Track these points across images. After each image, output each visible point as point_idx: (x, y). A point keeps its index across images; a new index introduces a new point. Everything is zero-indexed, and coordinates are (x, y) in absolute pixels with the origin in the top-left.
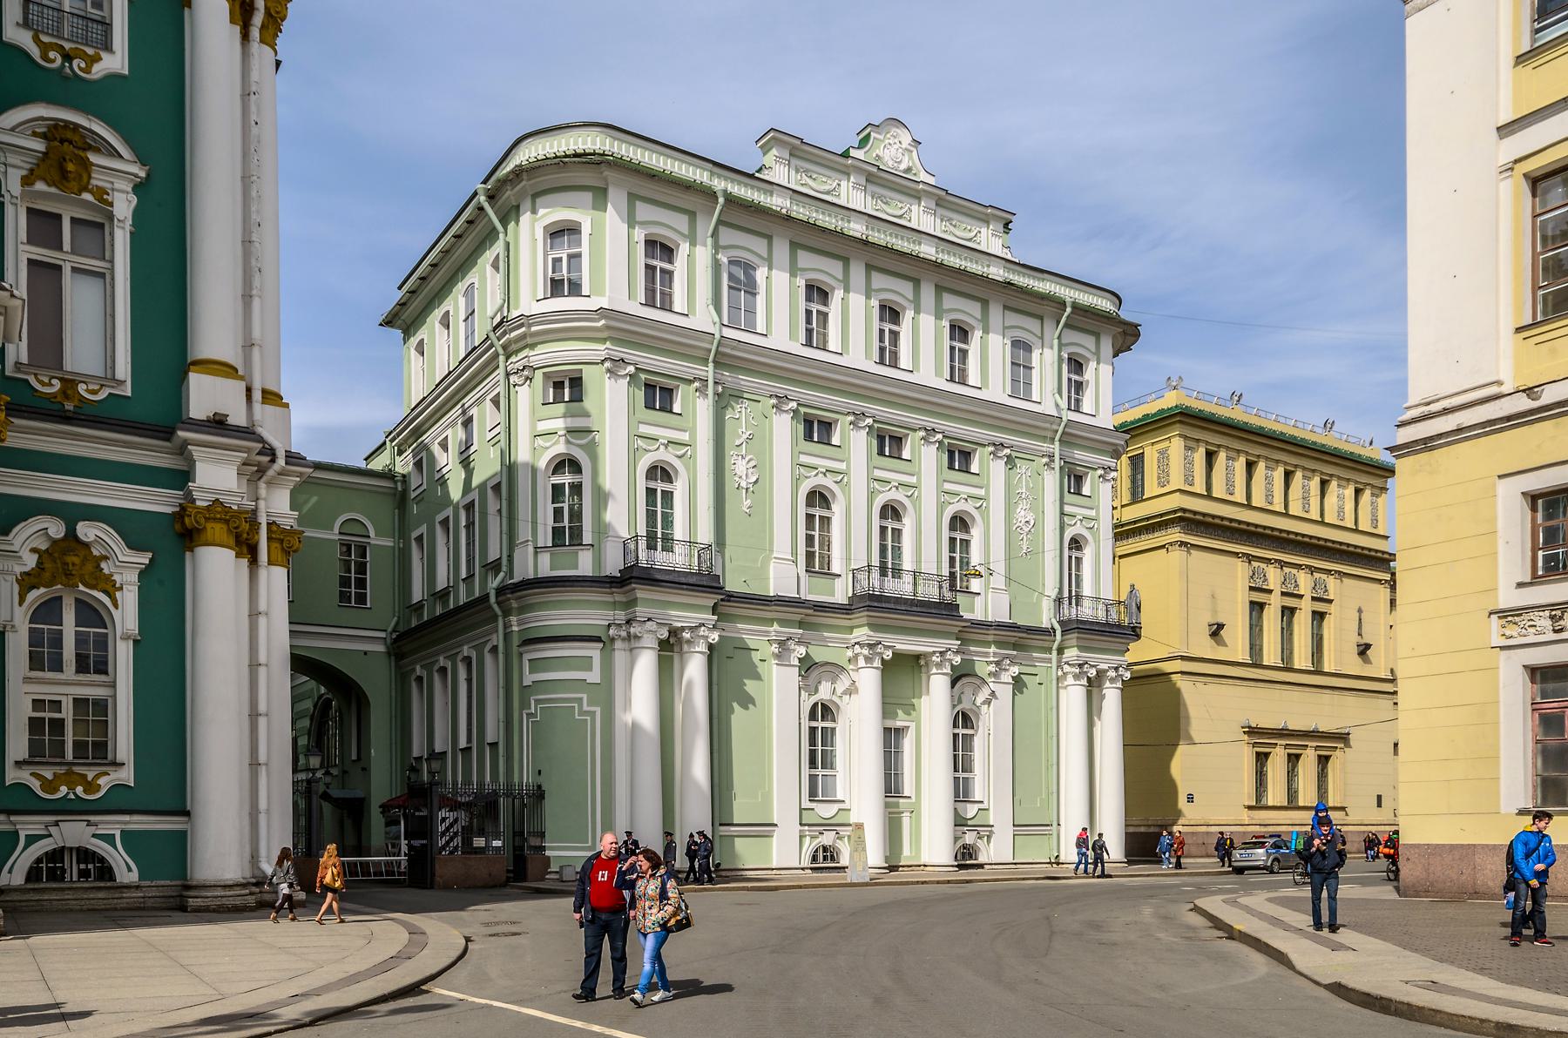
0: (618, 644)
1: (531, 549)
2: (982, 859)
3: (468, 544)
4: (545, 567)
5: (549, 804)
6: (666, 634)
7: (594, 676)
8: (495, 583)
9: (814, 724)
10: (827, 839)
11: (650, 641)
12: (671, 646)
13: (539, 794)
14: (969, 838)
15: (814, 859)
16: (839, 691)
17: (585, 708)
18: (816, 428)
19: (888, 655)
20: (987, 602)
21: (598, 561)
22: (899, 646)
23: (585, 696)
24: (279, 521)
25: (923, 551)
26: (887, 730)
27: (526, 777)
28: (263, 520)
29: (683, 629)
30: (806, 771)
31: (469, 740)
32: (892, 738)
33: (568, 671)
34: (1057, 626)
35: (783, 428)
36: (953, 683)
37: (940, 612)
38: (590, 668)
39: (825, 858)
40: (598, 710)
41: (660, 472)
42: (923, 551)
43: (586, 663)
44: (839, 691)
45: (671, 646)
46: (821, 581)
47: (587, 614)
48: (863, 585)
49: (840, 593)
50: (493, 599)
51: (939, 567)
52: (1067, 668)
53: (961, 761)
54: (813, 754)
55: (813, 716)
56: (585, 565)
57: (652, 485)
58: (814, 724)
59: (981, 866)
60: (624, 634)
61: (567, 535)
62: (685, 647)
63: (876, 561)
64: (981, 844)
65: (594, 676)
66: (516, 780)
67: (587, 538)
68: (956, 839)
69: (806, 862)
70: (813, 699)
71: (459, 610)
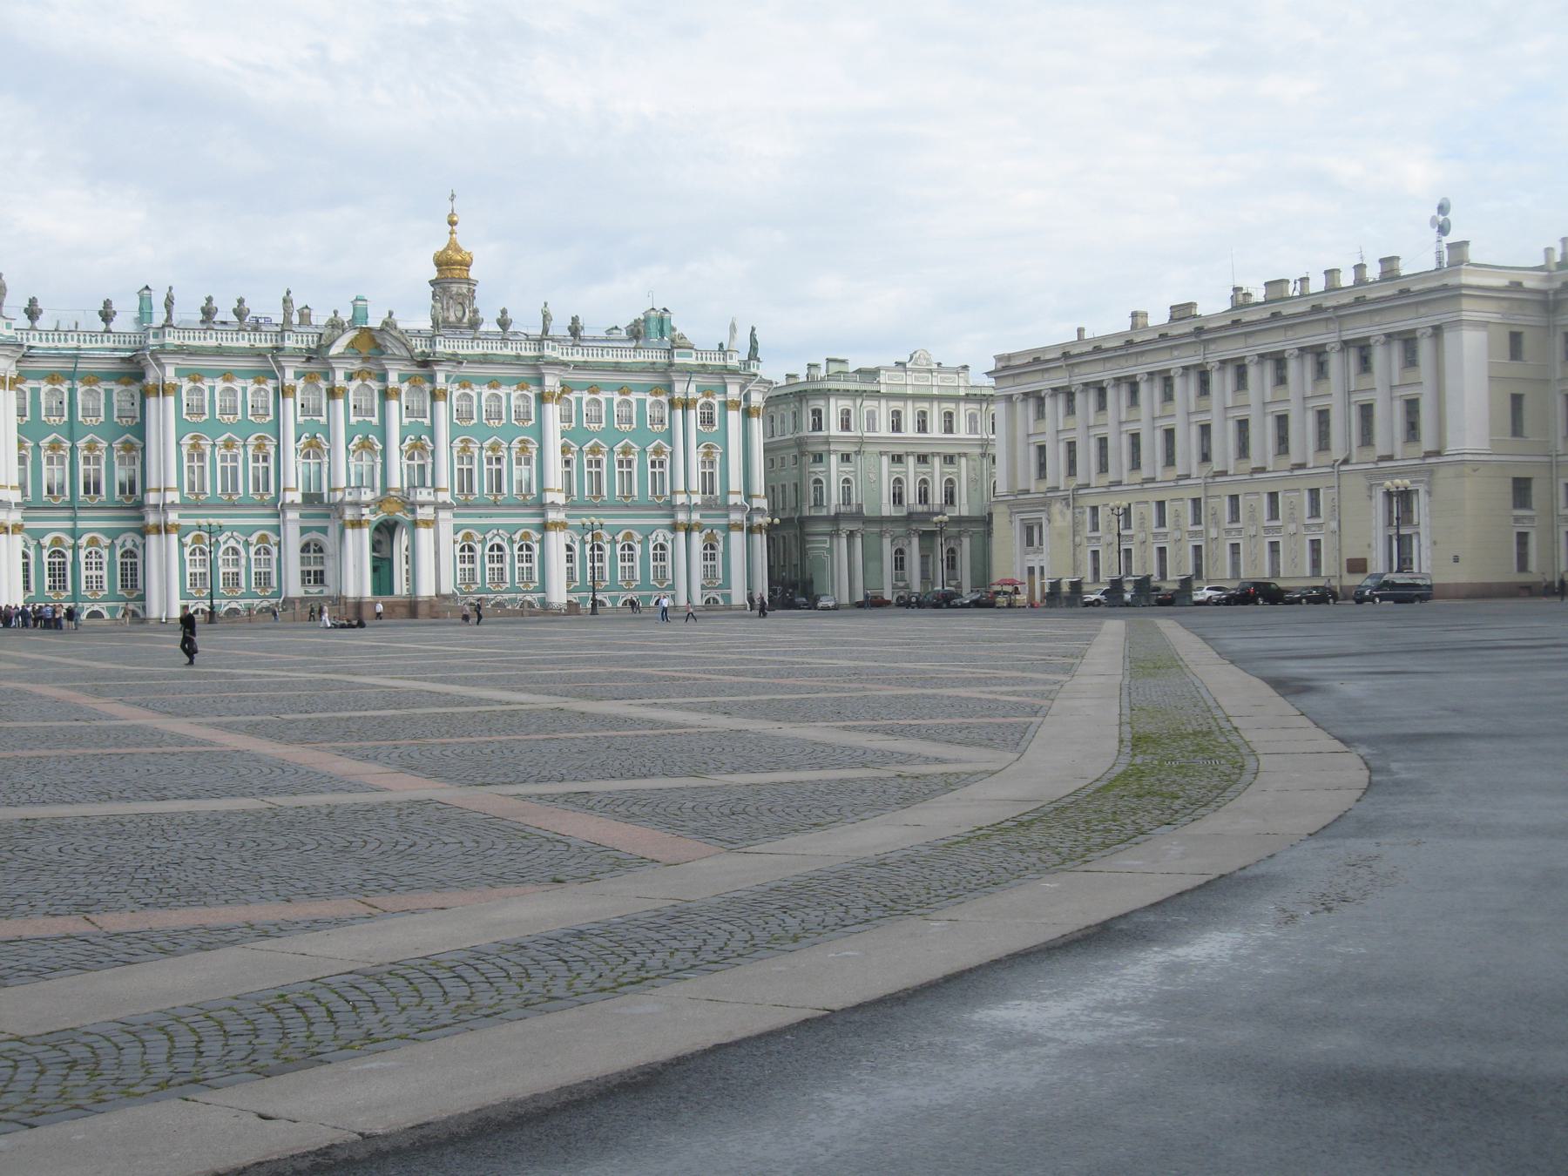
12: (851, 535)
13: (811, 582)
18: (897, 459)
25: (937, 496)
32: (924, 559)
33: (819, 545)
35: (885, 460)
41: (847, 481)
42: (937, 496)
45: (851, 535)
49: (905, 513)
56: (824, 513)
61: (818, 503)
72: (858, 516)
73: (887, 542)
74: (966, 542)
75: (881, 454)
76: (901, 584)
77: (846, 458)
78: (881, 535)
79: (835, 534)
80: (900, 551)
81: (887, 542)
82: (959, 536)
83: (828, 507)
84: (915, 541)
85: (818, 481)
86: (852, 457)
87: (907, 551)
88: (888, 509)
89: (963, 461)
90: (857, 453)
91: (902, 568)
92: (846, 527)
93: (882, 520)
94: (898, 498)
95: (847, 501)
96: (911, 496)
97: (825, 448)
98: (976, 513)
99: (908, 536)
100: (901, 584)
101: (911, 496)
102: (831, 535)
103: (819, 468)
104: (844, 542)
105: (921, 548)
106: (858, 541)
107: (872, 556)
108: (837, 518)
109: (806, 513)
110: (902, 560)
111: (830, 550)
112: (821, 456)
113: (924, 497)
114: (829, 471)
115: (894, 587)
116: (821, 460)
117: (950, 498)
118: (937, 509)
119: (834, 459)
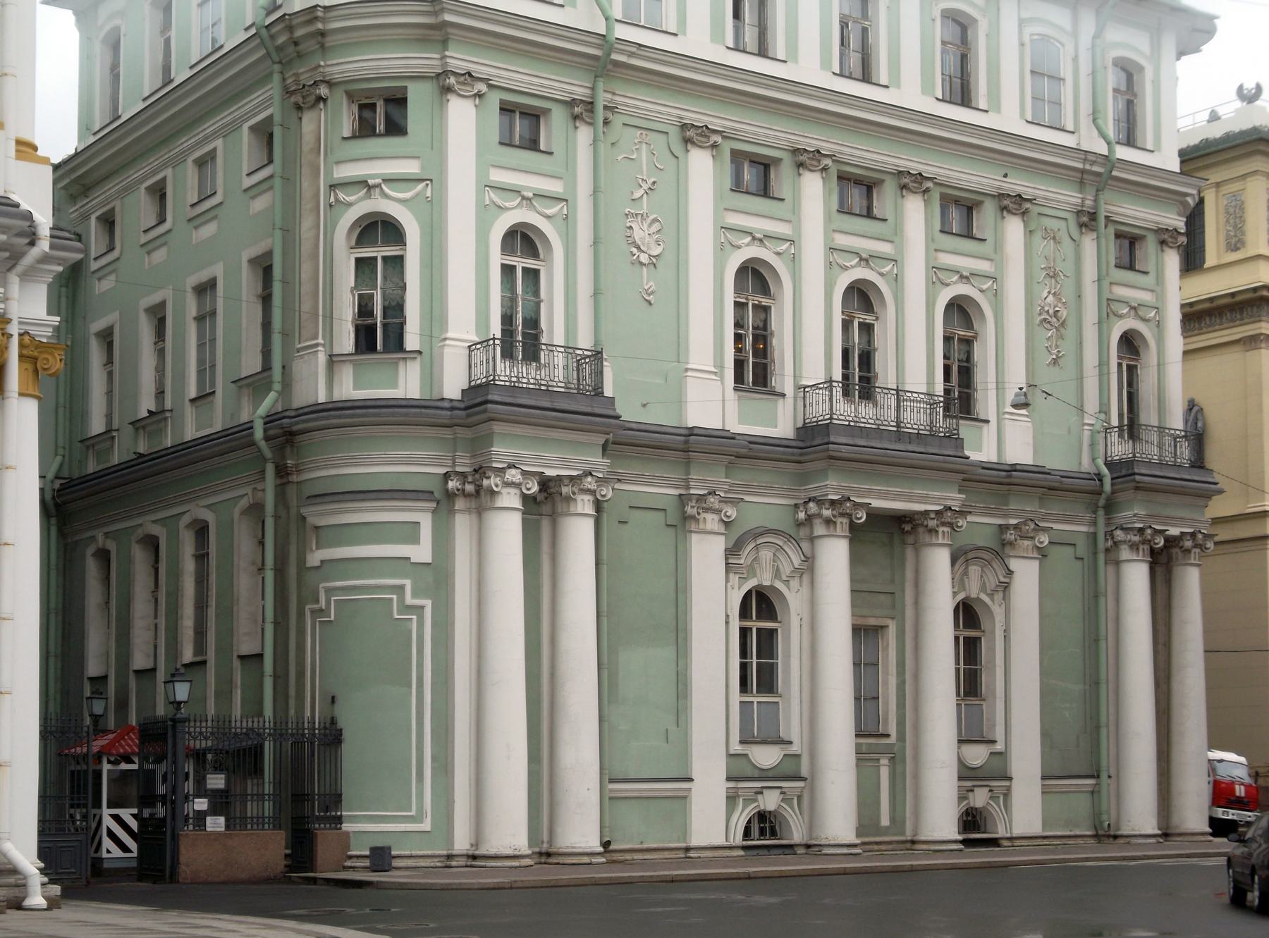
0: (460, 504)
1: (322, 358)
2: (1001, 832)
3: (201, 346)
4: (348, 388)
5: (350, 750)
6: (535, 488)
7: (422, 552)
8: (263, 410)
9: (747, 624)
10: (770, 801)
11: (510, 499)
12: (545, 502)
13: (333, 737)
14: (980, 798)
15: (747, 833)
16: (786, 569)
17: (409, 600)
19: (862, 516)
20: (1001, 439)
21: (432, 375)
22: (876, 503)
23: (408, 583)
24: (34, 331)
25: (912, 362)
26: (857, 630)
27: (313, 712)
28: (14, 329)
29: (559, 478)
30: (736, 696)
31: (200, 647)
33: (380, 547)
34: (1105, 471)
36: (954, 561)
37: (933, 454)
38: (414, 539)
39: (762, 832)
40: (428, 604)
42: (912, 360)
43: (410, 533)
44: (786, 569)
45: (545, 502)
46: (758, 402)
47: (417, 461)
48: (818, 410)
49: (780, 422)
50: (259, 433)
51: (930, 382)
52: (1119, 535)
53: (970, 684)
54: (744, 668)
55: (744, 612)
56: (408, 383)
57: (510, 261)
58: (747, 624)
59: (994, 842)
60: (470, 488)
61: (379, 335)
62: (560, 507)
63: (837, 375)
64: (996, 810)
65: (422, 552)
66: (308, 713)
67: (412, 341)
68: (961, 798)
69: (738, 839)
70: (751, 584)
71: (183, 448)
72: (582, 410)
73: (707, 553)
74: (1026, 575)
75: (692, 135)
76: (766, 757)
77: (523, 124)
78: (682, 520)
79: (468, 491)
80: (760, 604)
81: (707, 553)
82: (999, 550)
83: (430, 360)
84: (835, 555)
85: (380, 229)
86: (555, 128)
87: (794, 599)
88: (711, 404)
89: (1014, 228)
90: (581, 111)
91: (767, 681)
92: (521, 456)
93: (689, 446)
94: (754, 367)
95: (521, 336)
96: (809, 344)
97: (421, 60)
98: (1058, 461)
99: (801, 531)
100: (766, 757)
101: (809, 344)
102: (443, 501)
103: (382, 161)
104: (507, 529)
105: (858, 593)
106: (579, 535)
107: (640, 619)
108: (478, 408)
109: (317, 383)
110: (768, 641)
111: (437, 578)
112: (398, 101)
113: (860, 373)
114: (431, 181)
115: (740, 773)
116: (396, 128)
117: (960, 392)
118: (915, 418)
119: (464, 123)
